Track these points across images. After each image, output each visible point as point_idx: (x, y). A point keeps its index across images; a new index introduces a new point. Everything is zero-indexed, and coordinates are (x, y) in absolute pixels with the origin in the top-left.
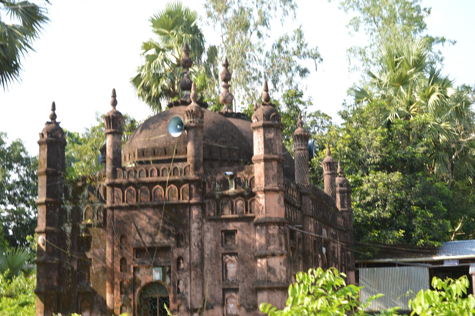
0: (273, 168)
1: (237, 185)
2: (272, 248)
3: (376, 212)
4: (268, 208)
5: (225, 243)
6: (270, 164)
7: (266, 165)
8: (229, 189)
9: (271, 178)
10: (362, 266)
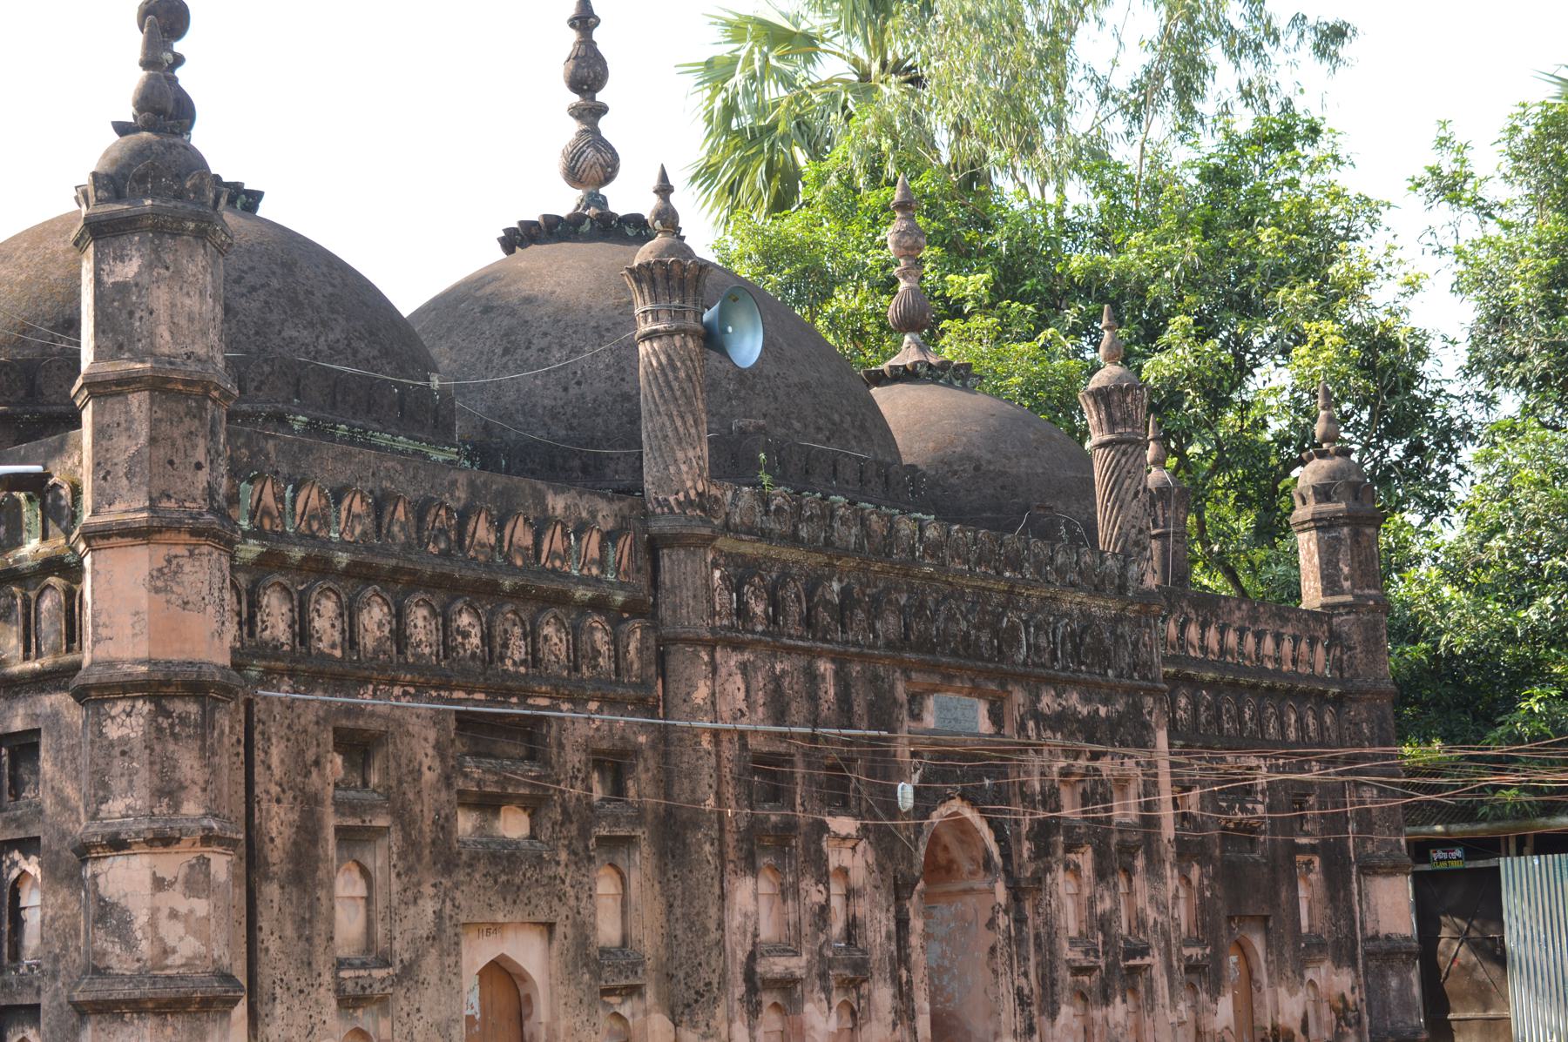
0: (131, 421)
1: (50, 522)
2: (116, 806)
3: (1548, 600)
4: (102, 619)
5: (17, 797)
6: (119, 407)
7: (102, 415)
8: (20, 544)
9: (121, 470)
10: (1513, 847)
